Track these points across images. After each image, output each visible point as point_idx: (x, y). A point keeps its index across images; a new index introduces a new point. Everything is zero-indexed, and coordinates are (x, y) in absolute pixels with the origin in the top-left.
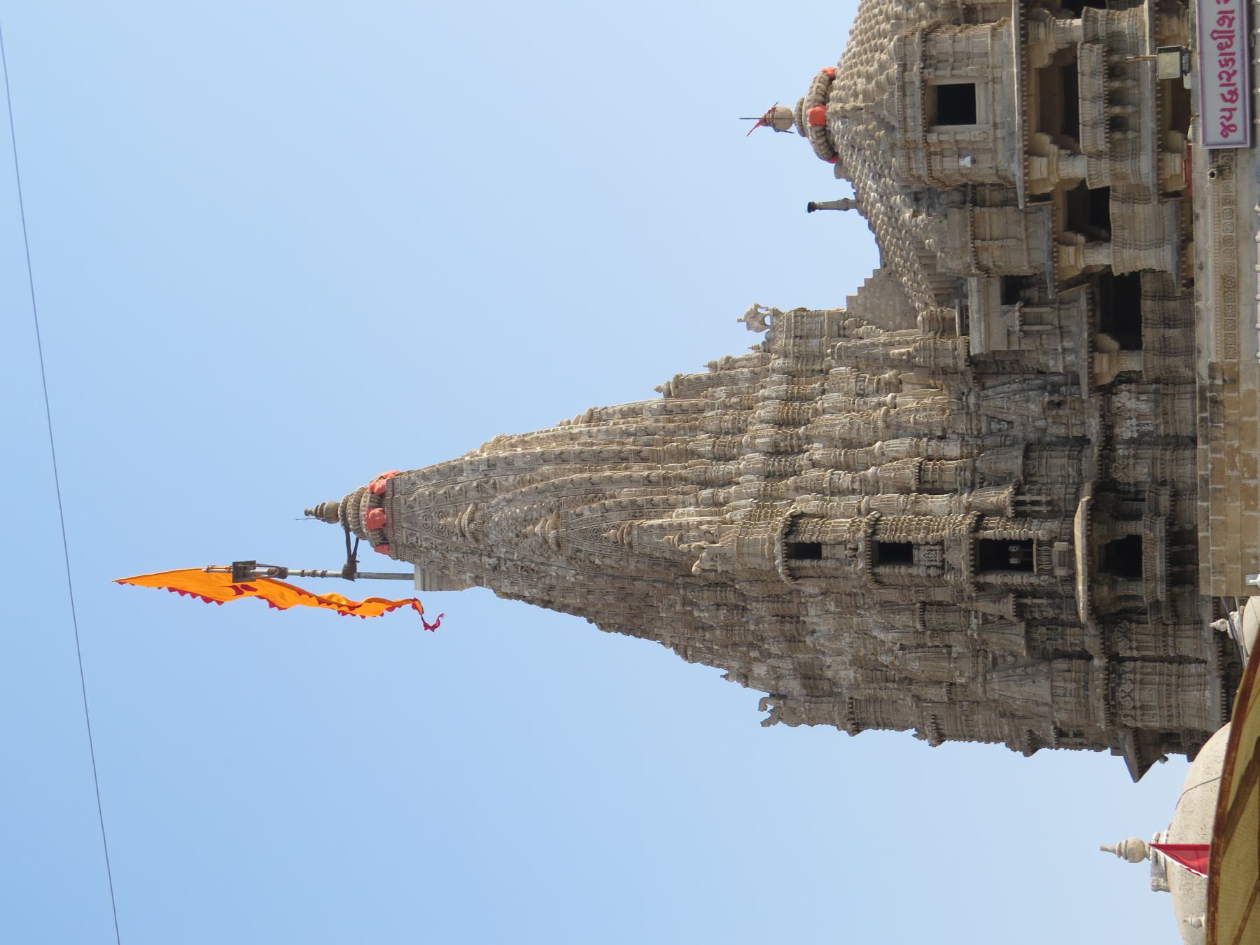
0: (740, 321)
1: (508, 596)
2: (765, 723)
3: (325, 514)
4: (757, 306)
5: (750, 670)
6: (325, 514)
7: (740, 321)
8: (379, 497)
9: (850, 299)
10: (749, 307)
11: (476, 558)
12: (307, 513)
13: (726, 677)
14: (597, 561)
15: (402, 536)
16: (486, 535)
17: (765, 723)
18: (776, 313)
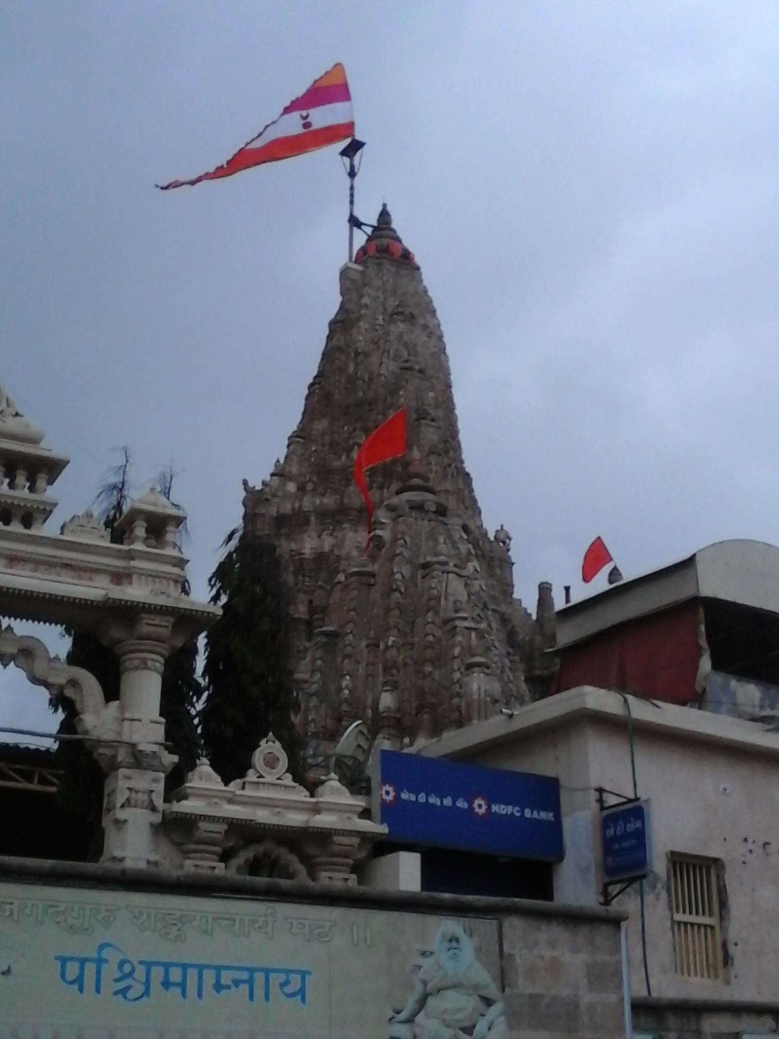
0: (502, 526)
1: (341, 325)
2: (245, 483)
3: (384, 216)
4: (510, 539)
5: (291, 479)
6: (384, 216)
7: (502, 526)
8: (406, 256)
9: (520, 601)
10: (511, 534)
11: (381, 309)
12: (385, 206)
13: (278, 461)
14: (401, 393)
15: (386, 264)
16: (402, 321)
17: (245, 483)
18: (508, 550)
